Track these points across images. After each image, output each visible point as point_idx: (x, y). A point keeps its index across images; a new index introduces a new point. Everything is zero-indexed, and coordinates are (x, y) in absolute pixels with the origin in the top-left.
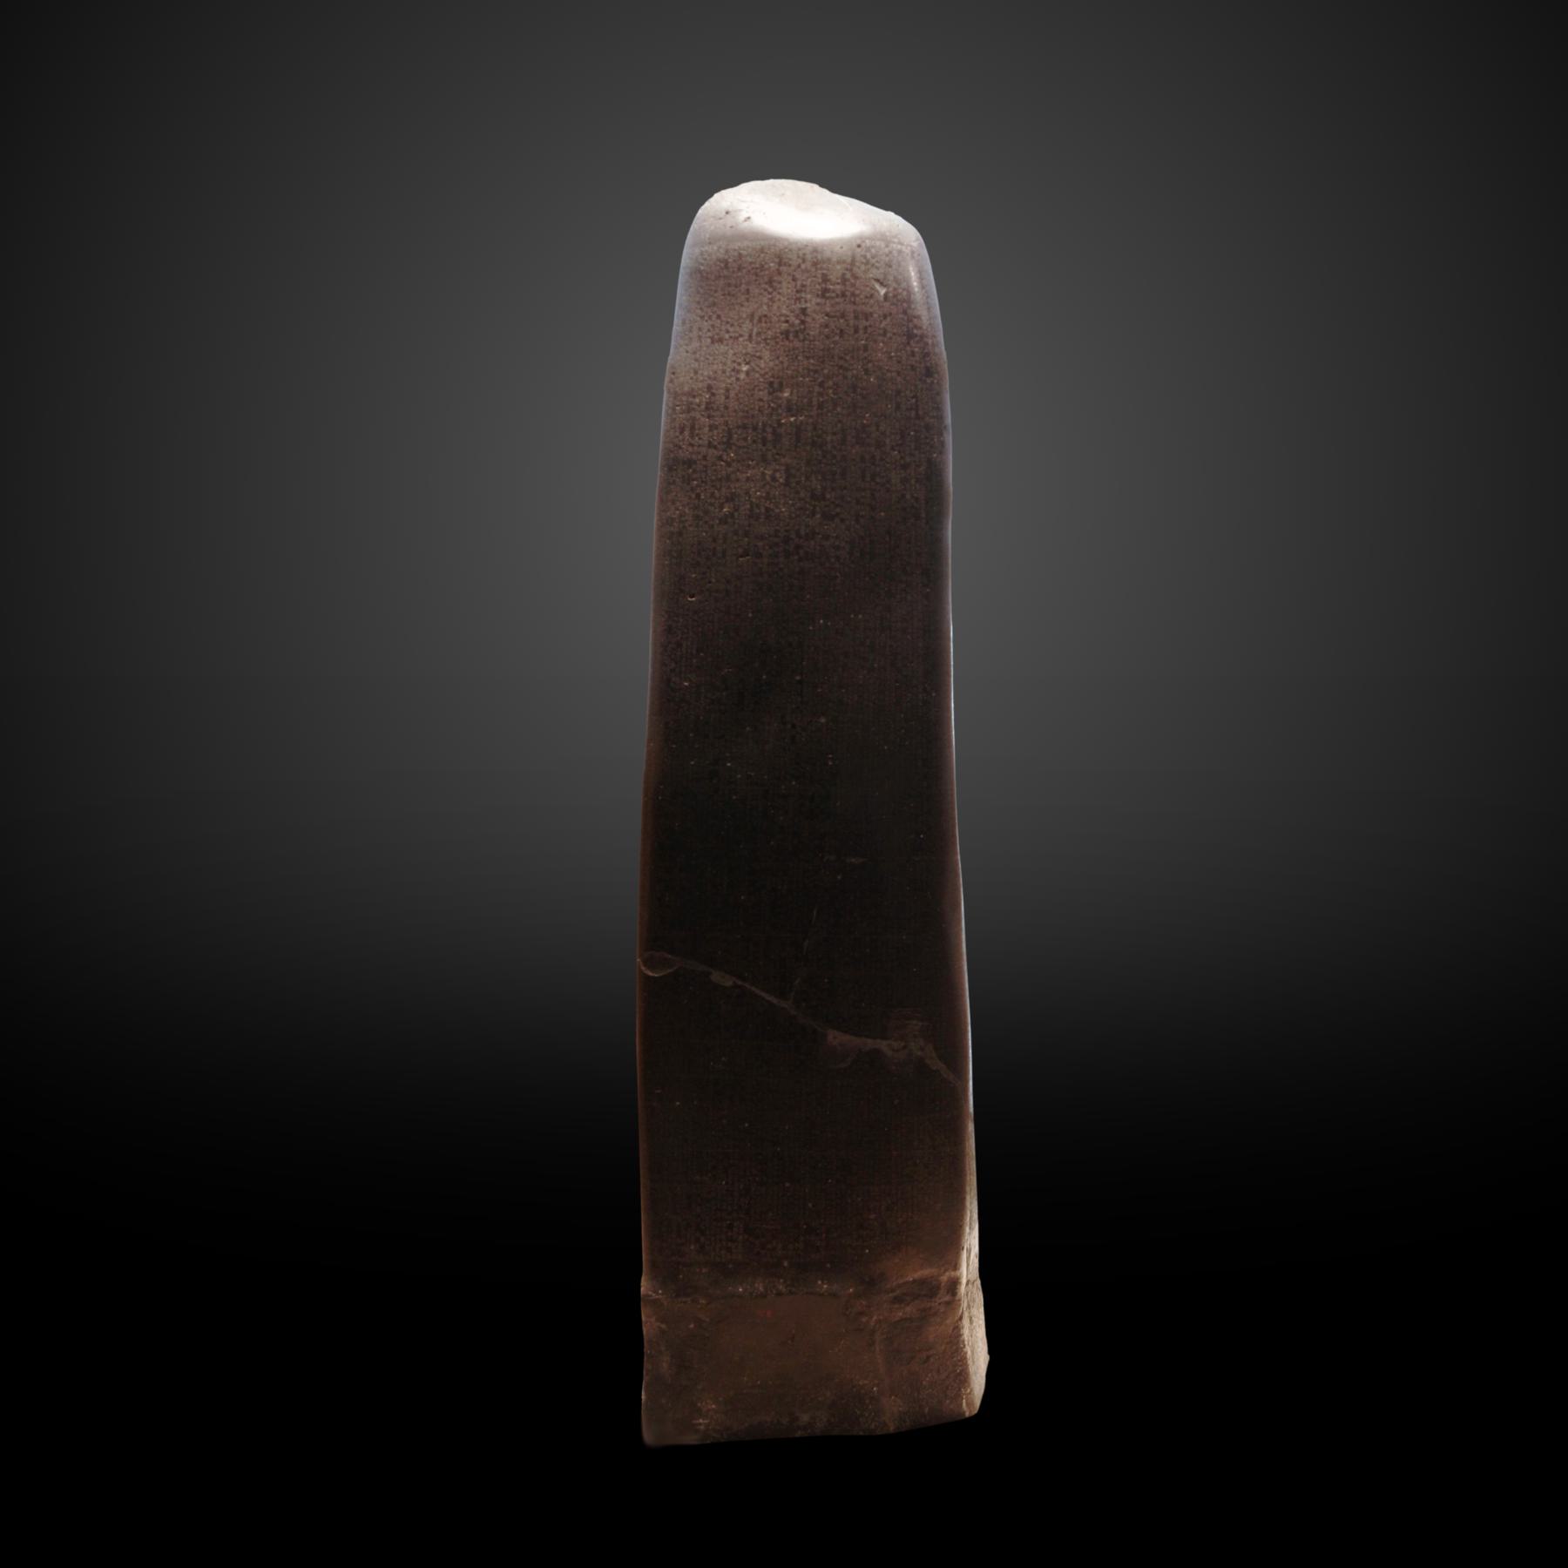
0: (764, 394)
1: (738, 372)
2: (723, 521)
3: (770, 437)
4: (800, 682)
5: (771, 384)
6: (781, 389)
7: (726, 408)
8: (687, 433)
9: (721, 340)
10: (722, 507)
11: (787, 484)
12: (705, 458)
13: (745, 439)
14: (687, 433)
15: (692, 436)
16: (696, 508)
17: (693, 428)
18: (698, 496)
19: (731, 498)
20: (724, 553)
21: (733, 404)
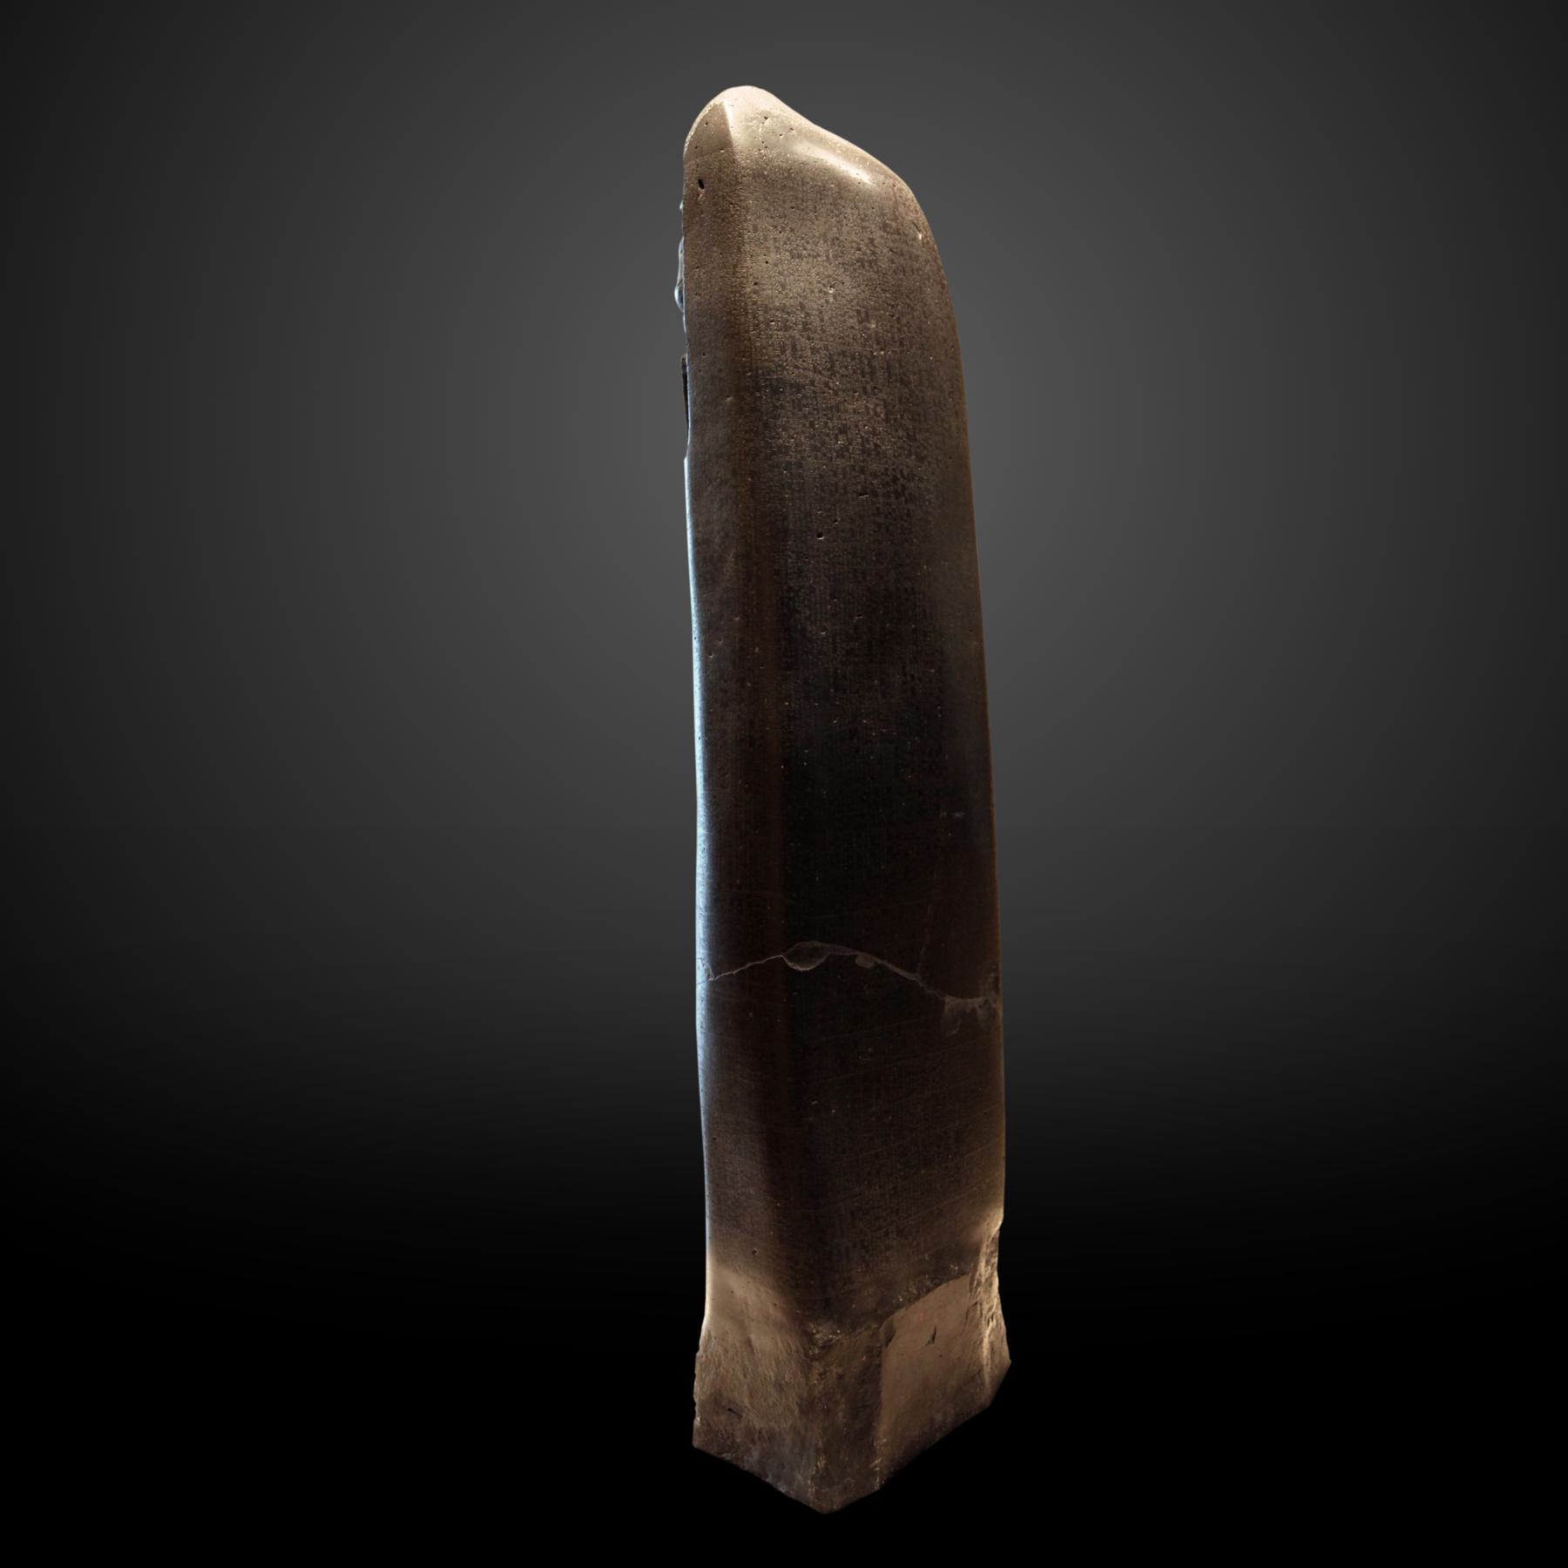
2: (840, 455)
3: (867, 369)
4: (915, 631)
5: (858, 312)
6: (867, 319)
9: (800, 256)
10: (837, 439)
11: (887, 420)
12: (812, 383)
16: (812, 437)
17: (794, 348)
18: (812, 424)
19: (843, 430)
20: (845, 488)
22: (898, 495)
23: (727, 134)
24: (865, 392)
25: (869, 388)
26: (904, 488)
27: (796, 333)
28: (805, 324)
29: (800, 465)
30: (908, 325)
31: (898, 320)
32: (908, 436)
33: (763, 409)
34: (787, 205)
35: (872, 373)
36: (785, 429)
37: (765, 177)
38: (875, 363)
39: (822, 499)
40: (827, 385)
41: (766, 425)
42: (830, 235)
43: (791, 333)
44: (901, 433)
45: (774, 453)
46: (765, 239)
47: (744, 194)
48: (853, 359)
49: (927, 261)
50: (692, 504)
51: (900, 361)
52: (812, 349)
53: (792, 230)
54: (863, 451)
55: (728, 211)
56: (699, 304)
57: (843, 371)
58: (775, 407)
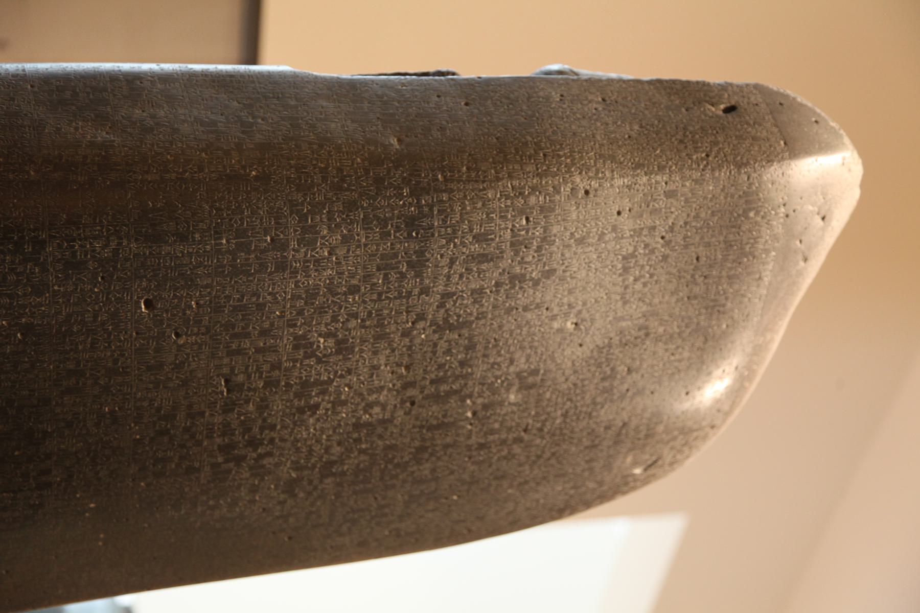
0: (521, 364)
1: (567, 315)
3: (444, 388)
5: (535, 372)
6: (525, 387)
7: (509, 311)
8: (476, 248)
9: (626, 270)
11: (357, 426)
12: (425, 291)
13: (448, 352)
14: (476, 248)
15: (472, 258)
17: (484, 258)
18: (354, 290)
19: (343, 348)
20: (239, 352)
21: (509, 323)
22: (225, 449)
23: (808, 151)
24: (406, 386)
25: (411, 392)
26: (239, 460)
27: (504, 264)
28: (522, 278)
29: (281, 266)
30: (510, 457)
31: (519, 440)
32: (332, 463)
33: (381, 202)
34: (702, 251)
35: (437, 398)
36: (346, 240)
37: (746, 212)
38: (453, 402)
39: (218, 309)
40: (421, 317)
41: (351, 206)
42: (653, 323)
43: (509, 253)
44: (336, 450)
45: (303, 218)
46: (654, 212)
47: (723, 174)
48: (462, 364)
49: (601, 483)
50: (205, 75)
51: (454, 445)
52: (480, 291)
53: (665, 258)
54: (305, 384)
55: (696, 149)
56: (548, 98)
57: (443, 345)
58: (383, 223)
